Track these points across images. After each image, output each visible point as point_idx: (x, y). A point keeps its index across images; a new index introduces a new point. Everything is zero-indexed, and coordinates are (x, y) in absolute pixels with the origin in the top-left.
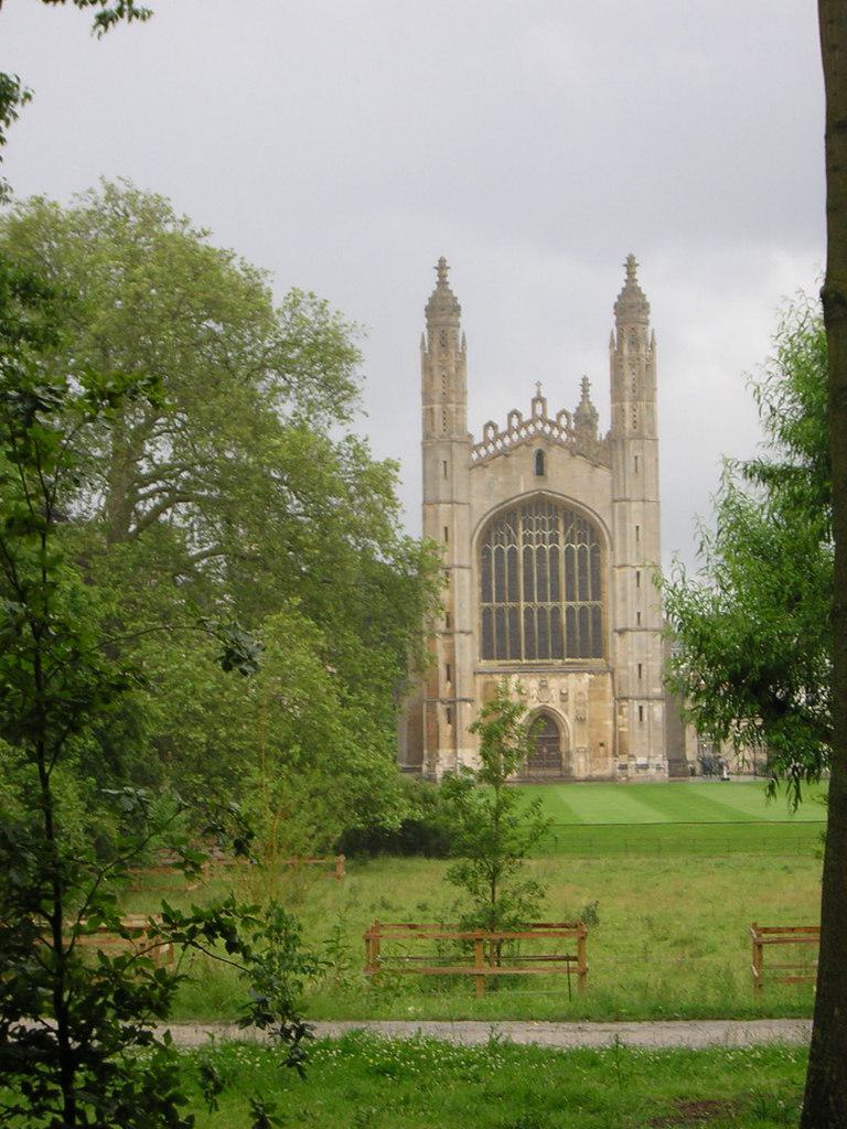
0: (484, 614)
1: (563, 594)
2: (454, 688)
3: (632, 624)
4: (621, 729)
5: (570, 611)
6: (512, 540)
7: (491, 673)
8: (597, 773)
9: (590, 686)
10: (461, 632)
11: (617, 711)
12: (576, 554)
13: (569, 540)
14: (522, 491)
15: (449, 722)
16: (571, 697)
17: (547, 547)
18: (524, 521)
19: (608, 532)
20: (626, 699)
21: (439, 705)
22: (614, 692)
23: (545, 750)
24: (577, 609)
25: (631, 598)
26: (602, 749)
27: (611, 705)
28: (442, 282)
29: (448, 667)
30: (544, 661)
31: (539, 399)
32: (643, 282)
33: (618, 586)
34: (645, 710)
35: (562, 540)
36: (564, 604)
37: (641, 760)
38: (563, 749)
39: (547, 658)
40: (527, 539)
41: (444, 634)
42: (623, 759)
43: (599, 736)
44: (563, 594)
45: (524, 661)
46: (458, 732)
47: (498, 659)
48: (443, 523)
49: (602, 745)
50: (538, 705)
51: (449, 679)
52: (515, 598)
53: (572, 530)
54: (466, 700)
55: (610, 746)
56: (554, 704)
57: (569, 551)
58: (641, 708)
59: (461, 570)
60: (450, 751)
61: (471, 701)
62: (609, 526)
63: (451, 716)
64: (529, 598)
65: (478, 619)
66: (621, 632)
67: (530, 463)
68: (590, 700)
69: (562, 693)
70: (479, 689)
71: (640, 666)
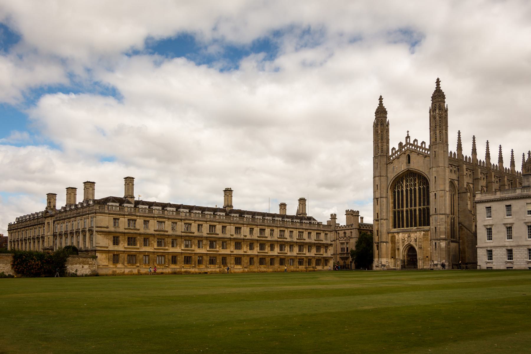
2: (379, 238)
5: (420, 210)
7: (393, 233)
9: (423, 236)
10: (381, 219)
12: (422, 190)
14: (403, 170)
15: (377, 250)
16: (418, 240)
17: (413, 188)
18: (406, 180)
21: (374, 244)
29: (377, 231)
34: (437, 244)
35: (417, 185)
36: (417, 208)
37: (435, 262)
39: (412, 227)
40: (407, 186)
41: (376, 220)
43: (426, 254)
45: (405, 228)
46: (380, 252)
47: (398, 228)
48: (376, 184)
49: (427, 257)
50: (407, 243)
51: (377, 235)
52: (403, 207)
53: (420, 181)
54: (384, 242)
55: (430, 257)
57: (420, 189)
58: (436, 243)
59: (382, 199)
60: (378, 259)
61: (386, 242)
64: (407, 206)
65: (391, 215)
66: (431, 216)
67: (404, 159)
68: (423, 241)
69: (415, 239)
70: (390, 238)
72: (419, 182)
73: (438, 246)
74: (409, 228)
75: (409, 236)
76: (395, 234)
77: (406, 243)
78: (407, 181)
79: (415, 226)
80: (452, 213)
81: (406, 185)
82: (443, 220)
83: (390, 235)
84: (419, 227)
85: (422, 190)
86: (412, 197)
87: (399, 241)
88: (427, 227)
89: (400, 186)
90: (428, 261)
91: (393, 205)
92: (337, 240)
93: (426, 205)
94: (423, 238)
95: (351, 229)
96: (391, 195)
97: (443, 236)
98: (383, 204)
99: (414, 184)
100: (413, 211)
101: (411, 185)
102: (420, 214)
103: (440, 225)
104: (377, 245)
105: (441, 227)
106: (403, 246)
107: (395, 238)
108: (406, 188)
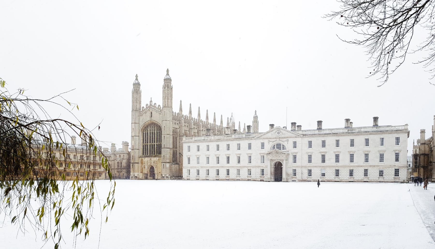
0: (143, 146)
5: (157, 144)
6: (148, 131)
13: (157, 130)
24: (158, 144)
31: (151, 101)
35: (156, 130)
36: (156, 144)
50: (150, 164)
56: (152, 164)
57: (157, 132)
58: (164, 165)
61: (138, 163)
64: (150, 142)
65: (142, 147)
70: (140, 161)
71: (164, 156)
78: (150, 127)
80: (176, 147)
82: (168, 152)
89: (147, 130)
91: (142, 141)
92: (115, 160)
95: (120, 154)
96: (142, 135)
97: (168, 161)
98: (137, 140)
101: (152, 130)
103: (166, 154)
104: (132, 165)
105: (167, 155)
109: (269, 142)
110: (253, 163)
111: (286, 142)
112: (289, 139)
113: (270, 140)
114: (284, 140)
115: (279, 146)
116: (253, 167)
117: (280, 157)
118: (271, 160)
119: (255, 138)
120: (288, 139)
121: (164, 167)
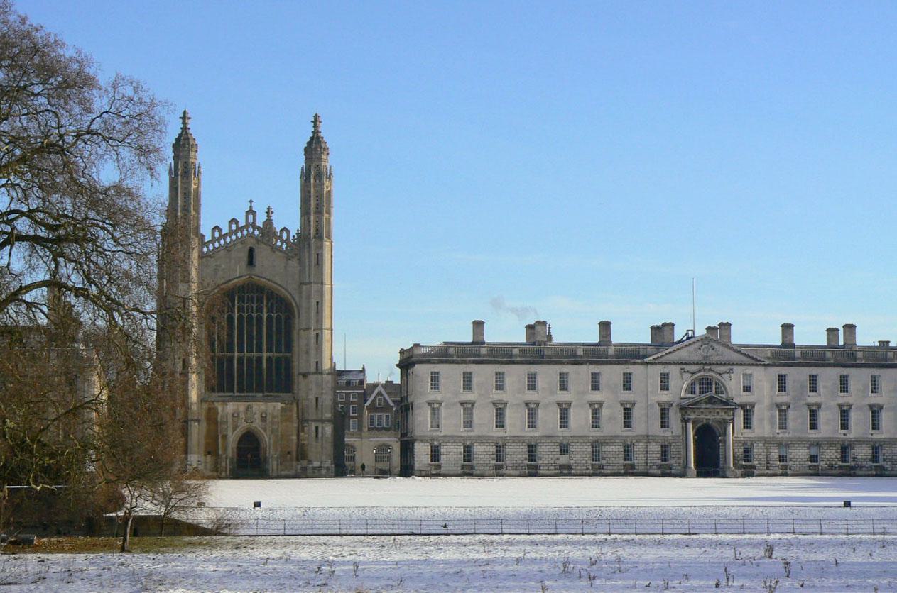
1: (265, 347)
3: (313, 369)
4: (303, 442)
5: (269, 359)
7: (213, 402)
8: (283, 473)
9: (282, 412)
11: (300, 429)
12: (274, 321)
14: (238, 276)
16: (269, 419)
17: (255, 315)
18: (239, 297)
19: (296, 303)
20: (307, 421)
22: (298, 417)
23: (249, 456)
24: (274, 358)
25: (313, 352)
26: (289, 456)
27: (296, 425)
28: (185, 129)
30: (250, 394)
31: (251, 212)
32: (324, 133)
33: (303, 342)
34: (320, 430)
35: (265, 310)
36: (265, 355)
37: (316, 464)
38: (261, 456)
42: (304, 463)
44: (265, 347)
45: (236, 394)
49: (289, 453)
53: (272, 304)
55: (294, 453)
56: (257, 425)
57: (269, 318)
58: (317, 428)
60: (183, 456)
61: (198, 421)
62: (297, 298)
63: (185, 432)
64: (241, 350)
66: (305, 375)
69: (262, 417)
71: (317, 399)
72: (270, 304)
73: (322, 433)
74: (246, 394)
75: (248, 409)
76: (216, 404)
77: (243, 426)
78: (241, 300)
79: (259, 390)
81: (238, 306)
83: (205, 406)
84: (268, 394)
85: (274, 321)
86: (252, 331)
87: (225, 420)
88: (284, 394)
90: (291, 460)
93: (283, 350)
94: (281, 416)
99: (257, 307)
100: (254, 362)
102: (269, 368)
106: (234, 429)
107: (218, 413)
108: (238, 313)
109: (683, 371)
110: (639, 427)
111: (725, 376)
112: (735, 368)
113: (684, 366)
114: (722, 369)
115: (705, 384)
116: (639, 439)
117: (718, 413)
118: (694, 422)
119: (647, 360)
120: (731, 367)
121: (320, 435)
